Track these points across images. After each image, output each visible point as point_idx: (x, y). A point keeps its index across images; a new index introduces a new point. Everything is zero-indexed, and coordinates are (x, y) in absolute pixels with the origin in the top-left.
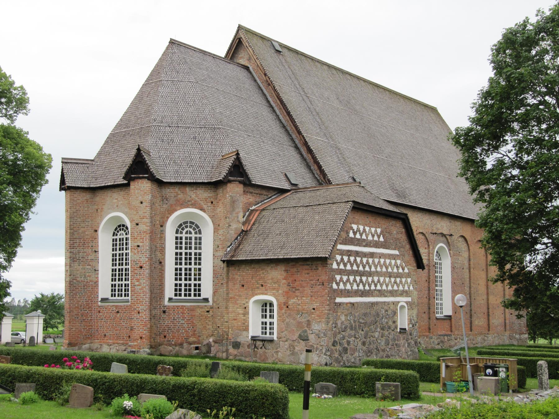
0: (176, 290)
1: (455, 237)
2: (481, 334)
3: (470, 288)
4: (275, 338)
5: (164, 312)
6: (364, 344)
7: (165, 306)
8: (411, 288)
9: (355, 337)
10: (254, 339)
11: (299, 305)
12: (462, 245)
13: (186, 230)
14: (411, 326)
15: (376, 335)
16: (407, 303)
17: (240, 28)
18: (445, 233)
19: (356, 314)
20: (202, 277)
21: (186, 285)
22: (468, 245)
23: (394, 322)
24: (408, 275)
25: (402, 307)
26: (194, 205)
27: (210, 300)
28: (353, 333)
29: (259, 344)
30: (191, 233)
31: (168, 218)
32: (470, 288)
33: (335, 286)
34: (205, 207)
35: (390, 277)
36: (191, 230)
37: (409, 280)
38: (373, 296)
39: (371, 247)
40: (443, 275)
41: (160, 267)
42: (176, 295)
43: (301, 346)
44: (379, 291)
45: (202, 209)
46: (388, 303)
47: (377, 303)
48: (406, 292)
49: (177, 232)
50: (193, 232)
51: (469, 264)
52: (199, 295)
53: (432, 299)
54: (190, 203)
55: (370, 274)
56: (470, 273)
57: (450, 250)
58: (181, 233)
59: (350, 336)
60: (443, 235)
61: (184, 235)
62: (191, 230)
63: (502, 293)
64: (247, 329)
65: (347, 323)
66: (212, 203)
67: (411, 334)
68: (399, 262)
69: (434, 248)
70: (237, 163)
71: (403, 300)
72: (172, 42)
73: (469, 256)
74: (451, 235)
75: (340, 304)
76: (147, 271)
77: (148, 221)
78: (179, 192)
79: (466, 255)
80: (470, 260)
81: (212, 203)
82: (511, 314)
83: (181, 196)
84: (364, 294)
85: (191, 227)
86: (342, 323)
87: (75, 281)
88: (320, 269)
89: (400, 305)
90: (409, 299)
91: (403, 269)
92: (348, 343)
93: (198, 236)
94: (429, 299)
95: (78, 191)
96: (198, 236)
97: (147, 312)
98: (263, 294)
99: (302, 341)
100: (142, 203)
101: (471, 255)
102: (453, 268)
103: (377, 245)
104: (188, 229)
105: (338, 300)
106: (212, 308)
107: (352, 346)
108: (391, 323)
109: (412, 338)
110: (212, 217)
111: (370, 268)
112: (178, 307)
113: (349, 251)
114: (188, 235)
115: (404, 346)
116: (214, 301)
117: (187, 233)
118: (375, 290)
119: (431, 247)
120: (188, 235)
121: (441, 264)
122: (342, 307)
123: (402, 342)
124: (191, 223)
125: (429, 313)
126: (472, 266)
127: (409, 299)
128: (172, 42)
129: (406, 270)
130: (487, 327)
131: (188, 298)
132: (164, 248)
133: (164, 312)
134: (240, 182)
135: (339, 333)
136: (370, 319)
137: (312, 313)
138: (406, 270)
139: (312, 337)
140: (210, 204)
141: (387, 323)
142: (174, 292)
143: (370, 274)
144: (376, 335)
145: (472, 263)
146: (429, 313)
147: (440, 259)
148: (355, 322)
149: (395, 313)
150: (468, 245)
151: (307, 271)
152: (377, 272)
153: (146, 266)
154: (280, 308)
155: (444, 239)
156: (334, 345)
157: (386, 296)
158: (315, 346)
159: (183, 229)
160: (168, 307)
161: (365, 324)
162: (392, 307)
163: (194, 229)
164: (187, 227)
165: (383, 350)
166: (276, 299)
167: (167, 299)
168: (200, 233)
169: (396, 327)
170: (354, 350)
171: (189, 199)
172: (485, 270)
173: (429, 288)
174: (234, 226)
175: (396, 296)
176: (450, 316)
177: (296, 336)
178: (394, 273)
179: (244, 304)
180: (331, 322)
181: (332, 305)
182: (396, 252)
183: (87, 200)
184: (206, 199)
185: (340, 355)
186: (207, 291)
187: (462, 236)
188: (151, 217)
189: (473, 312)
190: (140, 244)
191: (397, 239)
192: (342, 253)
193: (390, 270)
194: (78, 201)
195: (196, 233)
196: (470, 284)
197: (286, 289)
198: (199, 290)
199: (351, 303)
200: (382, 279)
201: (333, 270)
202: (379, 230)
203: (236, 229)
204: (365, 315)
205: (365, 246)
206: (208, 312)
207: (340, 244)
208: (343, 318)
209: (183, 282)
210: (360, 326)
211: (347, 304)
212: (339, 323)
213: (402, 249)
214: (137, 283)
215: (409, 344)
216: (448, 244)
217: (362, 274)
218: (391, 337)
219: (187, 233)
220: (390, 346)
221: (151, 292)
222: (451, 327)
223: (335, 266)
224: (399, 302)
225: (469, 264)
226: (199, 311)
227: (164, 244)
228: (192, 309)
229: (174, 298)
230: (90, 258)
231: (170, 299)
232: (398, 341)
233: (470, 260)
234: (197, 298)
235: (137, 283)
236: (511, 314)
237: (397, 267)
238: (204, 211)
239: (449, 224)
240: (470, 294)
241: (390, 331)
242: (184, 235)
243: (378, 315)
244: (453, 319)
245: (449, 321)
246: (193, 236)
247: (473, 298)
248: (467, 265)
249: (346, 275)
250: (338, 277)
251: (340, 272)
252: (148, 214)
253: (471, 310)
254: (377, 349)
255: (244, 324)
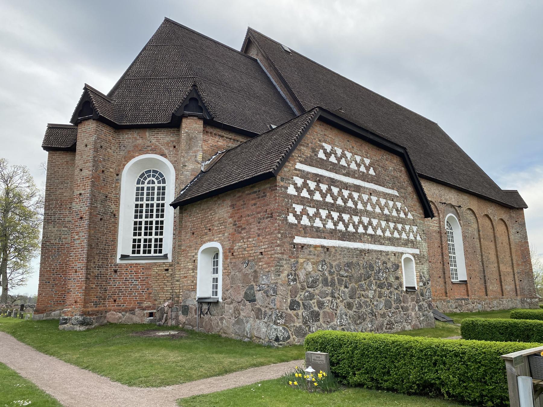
0: (134, 246)
1: (464, 209)
2: (496, 298)
3: (482, 256)
4: (220, 300)
5: (116, 271)
6: (349, 306)
7: (116, 265)
8: (418, 238)
9: (333, 297)
10: (201, 301)
11: (245, 249)
12: (471, 218)
13: (148, 179)
14: (421, 284)
15: (371, 294)
16: (414, 255)
17: (250, 31)
18: (453, 204)
19: (334, 264)
20: (164, 231)
21: (145, 240)
22: (476, 217)
23: (397, 278)
24: (413, 223)
25: (407, 260)
26: (154, 151)
27: (170, 256)
28: (329, 290)
29: (205, 307)
30: (153, 182)
31: (124, 165)
32: (482, 256)
33: (291, 219)
34: (166, 152)
35: (387, 221)
36: (154, 179)
37: (415, 228)
38: (361, 241)
39: (356, 178)
40: (455, 243)
41: (113, 220)
42: (134, 252)
43: (247, 310)
44: (371, 235)
45: (163, 155)
46: (387, 253)
47: (369, 251)
48: (412, 242)
49: (138, 183)
50: (156, 181)
51: (479, 235)
52: (160, 252)
53: (446, 264)
54: (149, 148)
55: (355, 212)
56: (480, 243)
57: (459, 220)
58: (143, 183)
59: (324, 295)
60: (453, 206)
61: (146, 185)
62: (154, 179)
63: (511, 262)
64: (194, 290)
65: (316, 275)
66: (175, 147)
67: (422, 295)
68: (399, 205)
69: (444, 217)
70: (195, 96)
71: (408, 252)
72: (167, 20)
73: (478, 227)
74: (460, 207)
75: (303, 246)
76: (86, 222)
77: (90, 164)
78: (138, 137)
79: (475, 226)
80: (479, 231)
81: (175, 147)
82: (521, 281)
83: (140, 141)
84: (345, 236)
85: (154, 176)
86: (308, 274)
87: (48, 244)
88: (268, 194)
89: (404, 256)
90: (417, 251)
91: (406, 214)
92: (321, 305)
93: (162, 185)
94: (444, 265)
95: (58, 153)
96: (162, 185)
97: (84, 271)
98: (210, 240)
99: (248, 303)
100: (86, 146)
101: (480, 227)
102: (464, 237)
103: (364, 177)
104: (151, 178)
105: (298, 240)
106: (171, 265)
107: (327, 310)
108: (392, 279)
109: (424, 300)
110: (174, 163)
111: (356, 204)
112: (131, 265)
113: (317, 175)
114: (151, 185)
115: (413, 309)
116: (173, 257)
117: (148, 183)
118: (366, 234)
119: (441, 216)
120: (151, 185)
121: (452, 233)
122: (306, 251)
123: (410, 304)
124: (154, 171)
125: (444, 278)
126: (481, 236)
127: (417, 251)
128: (167, 20)
129: (410, 216)
130: (501, 292)
131: (147, 255)
132: (119, 199)
133: (116, 271)
134: (200, 118)
135: (303, 289)
136: (356, 273)
137: (260, 260)
138: (410, 216)
139: (259, 295)
140: (172, 149)
141: (387, 279)
142: (131, 249)
143: (355, 212)
144: (371, 294)
145: (481, 233)
146: (444, 278)
147: (451, 229)
148: (331, 273)
149: (397, 267)
150: (476, 217)
151: (253, 202)
152: (367, 211)
153: (86, 217)
154: (225, 257)
155: (453, 210)
156: (292, 309)
157: (382, 244)
158: (263, 310)
159: (145, 179)
160: (121, 265)
161: (350, 277)
162: (392, 259)
163: (157, 178)
164: (149, 176)
165: (383, 316)
166: (222, 245)
167: (119, 256)
168: (164, 182)
169: (401, 285)
170: (331, 317)
171: (149, 143)
172: (493, 241)
173: (442, 254)
174: (190, 166)
175: (398, 246)
176: (466, 281)
177: (241, 297)
178: (393, 217)
179: (193, 256)
180: (286, 273)
181: (287, 246)
182: (396, 193)
183: (67, 162)
184: (168, 143)
185: (305, 323)
186: (168, 247)
187: (470, 209)
188: (95, 161)
189: (487, 278)
190: (83, 192)
191: (394, 177)
192: (305, 176)
193: (386, 212)
194: (57, 163)
195: (159, 182)
196: (481, 252)
197: (231, 229)
198: (161, 246)
199: (323, 247)
200: (375, 222)
201: (290, 196)
202: (367, 161)
203: (193, 170)
204: (349, 265)
205: (344, 175)
206: (167, 270)
207: (301, 162)
208: (310, 268)
209: (143, 237)
210: (340, 282)
211: (316, 247)
212: (302, 275)
213: (402, 190)
214: (77, 237)
215: (420, 308)
216: (458, 215)
217: (341, 210)
218: (394, 297)
219: (148, 183)
220: (393, 310)
221: (90, 245)
222: (467, 291)
223: (291, 190)
224: (402, 253)
225: (479, 235)
226: (156, 269)
227: (119, 194)
228: (148, 267)
229: (131, 255)
230: (67, 219)
231: (124, 257)
232: (404, 302)
233: (479, 231)
234: (158, 254)
235: (77, 237)
236: (521, 281)
237: (397, 210)
238: (166, 157)
239: (456, 196)
240: (482, 261)
241: (392, 289)
242: (146, 185)
243: (371, 267)
244: (468, 284)
245: (464, 286)
246: (156, 185)
247: (485, 265)
248: (477, 235)
249: (314, 207)
250: (298, 208)
251: (302, 201)
252: (90, 158)
253: (485, 276)
254: (372, 313)
255: (193, 282)
